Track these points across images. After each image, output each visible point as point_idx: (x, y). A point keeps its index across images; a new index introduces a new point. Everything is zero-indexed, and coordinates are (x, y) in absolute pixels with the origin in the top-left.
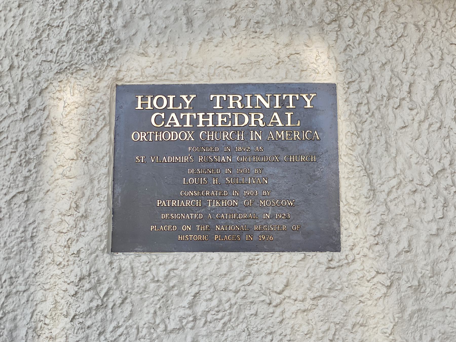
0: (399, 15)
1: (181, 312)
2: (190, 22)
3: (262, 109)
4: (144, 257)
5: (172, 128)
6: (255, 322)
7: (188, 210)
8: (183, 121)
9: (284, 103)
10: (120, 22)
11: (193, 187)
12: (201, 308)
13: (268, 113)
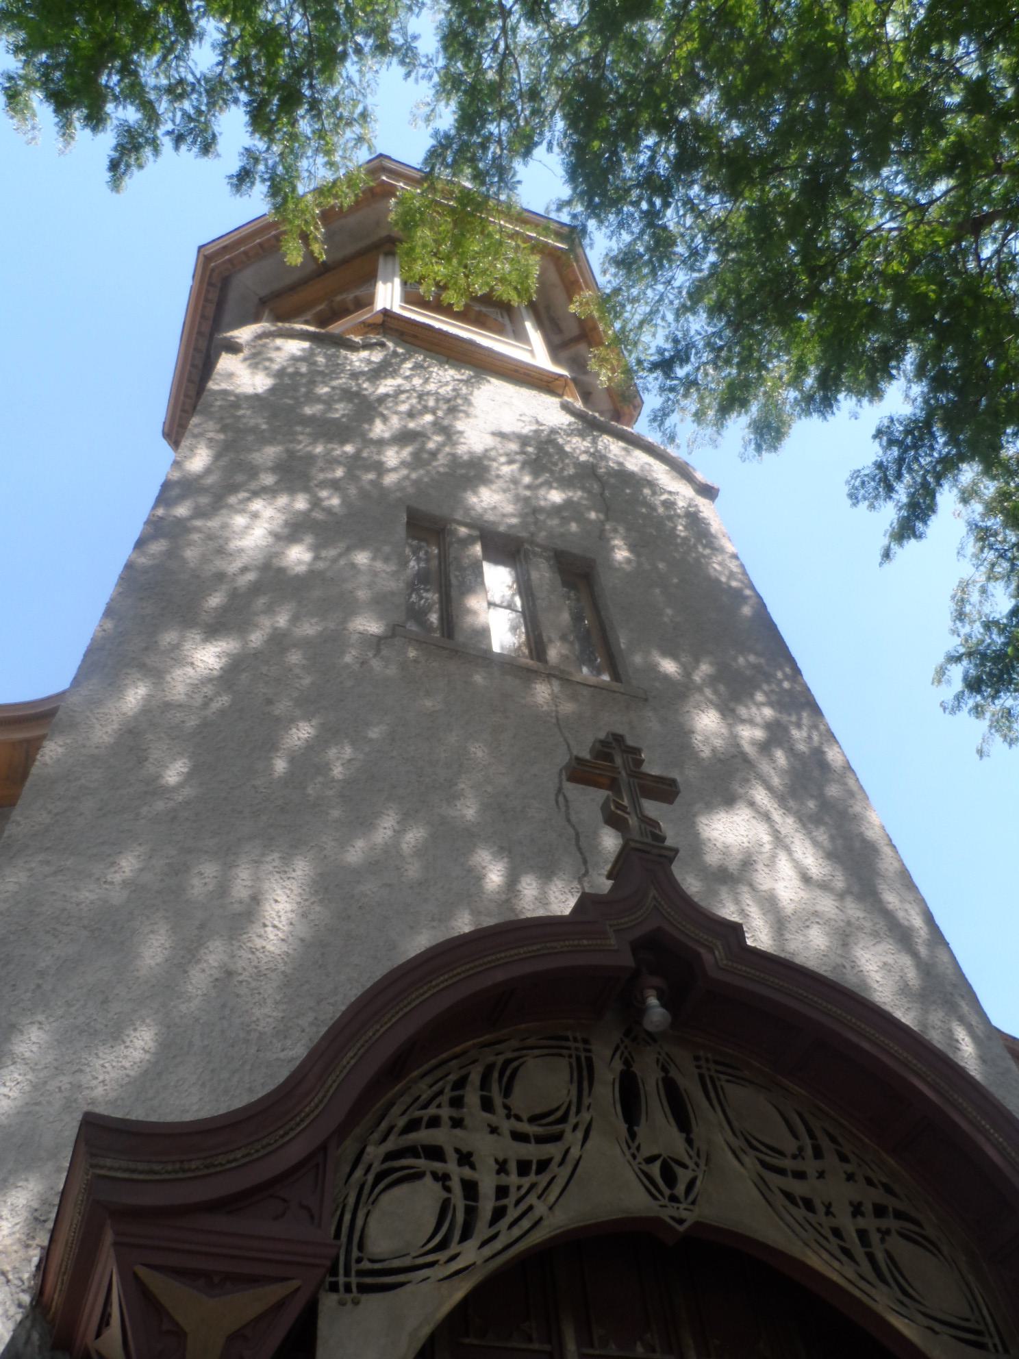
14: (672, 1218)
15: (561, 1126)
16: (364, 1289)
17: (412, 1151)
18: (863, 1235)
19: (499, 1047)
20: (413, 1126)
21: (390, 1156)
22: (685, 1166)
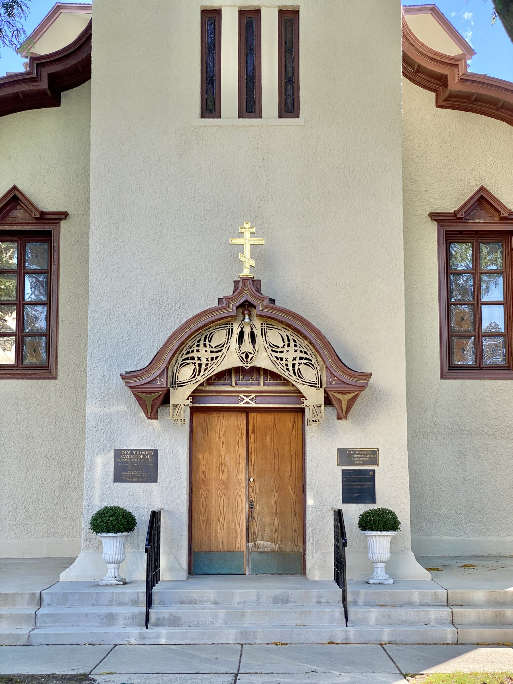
0: (171, 436)
1: (127, 494)
2: (129, 436)
3: (143, 454)
4: (120, 483)
5: (126, 458)
6: (141, 496)
7: (128, 474)
8: (128, 457)
9: (148, 453)
10: (115, 436)
11: (129, 470)
12: (130, 494)
13: (144, 455)
14: (245, 366)
15: (222, 348)
16: (178, 386)
17: (187, 359)
18: (294, 365)
19: (209, 330)
20: (188, 353)
21: (183, 360)
22: (251, 353)
